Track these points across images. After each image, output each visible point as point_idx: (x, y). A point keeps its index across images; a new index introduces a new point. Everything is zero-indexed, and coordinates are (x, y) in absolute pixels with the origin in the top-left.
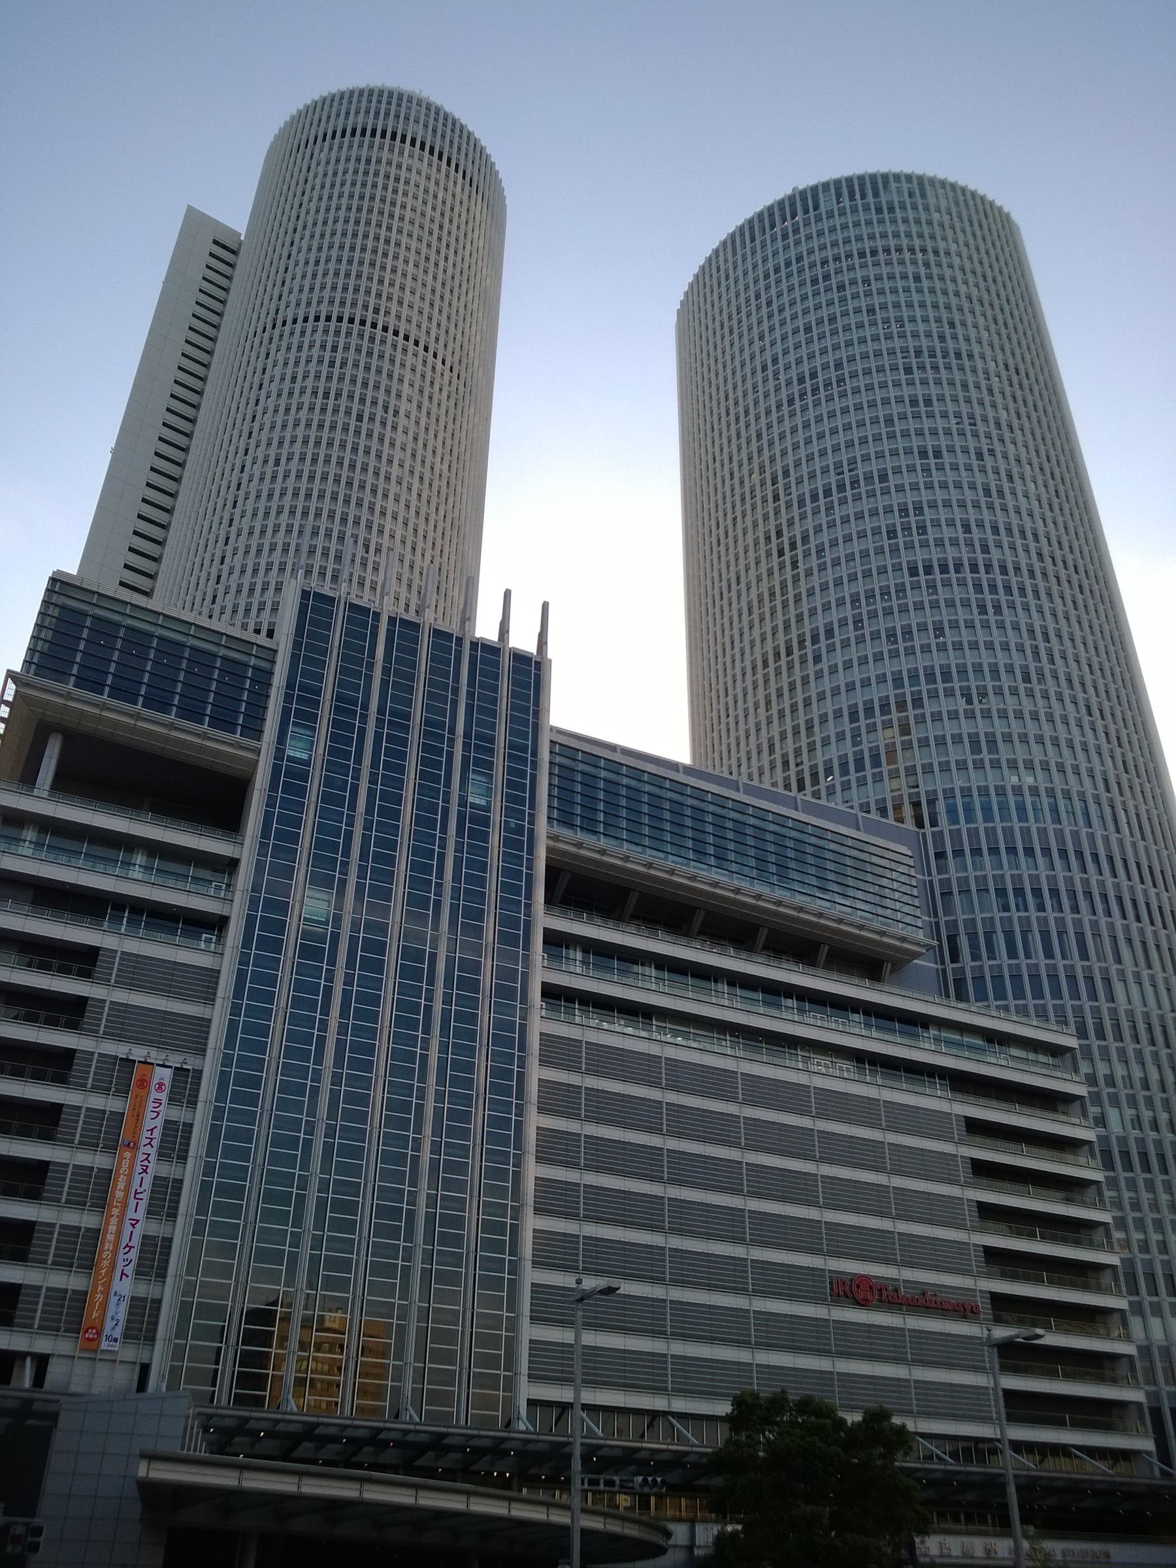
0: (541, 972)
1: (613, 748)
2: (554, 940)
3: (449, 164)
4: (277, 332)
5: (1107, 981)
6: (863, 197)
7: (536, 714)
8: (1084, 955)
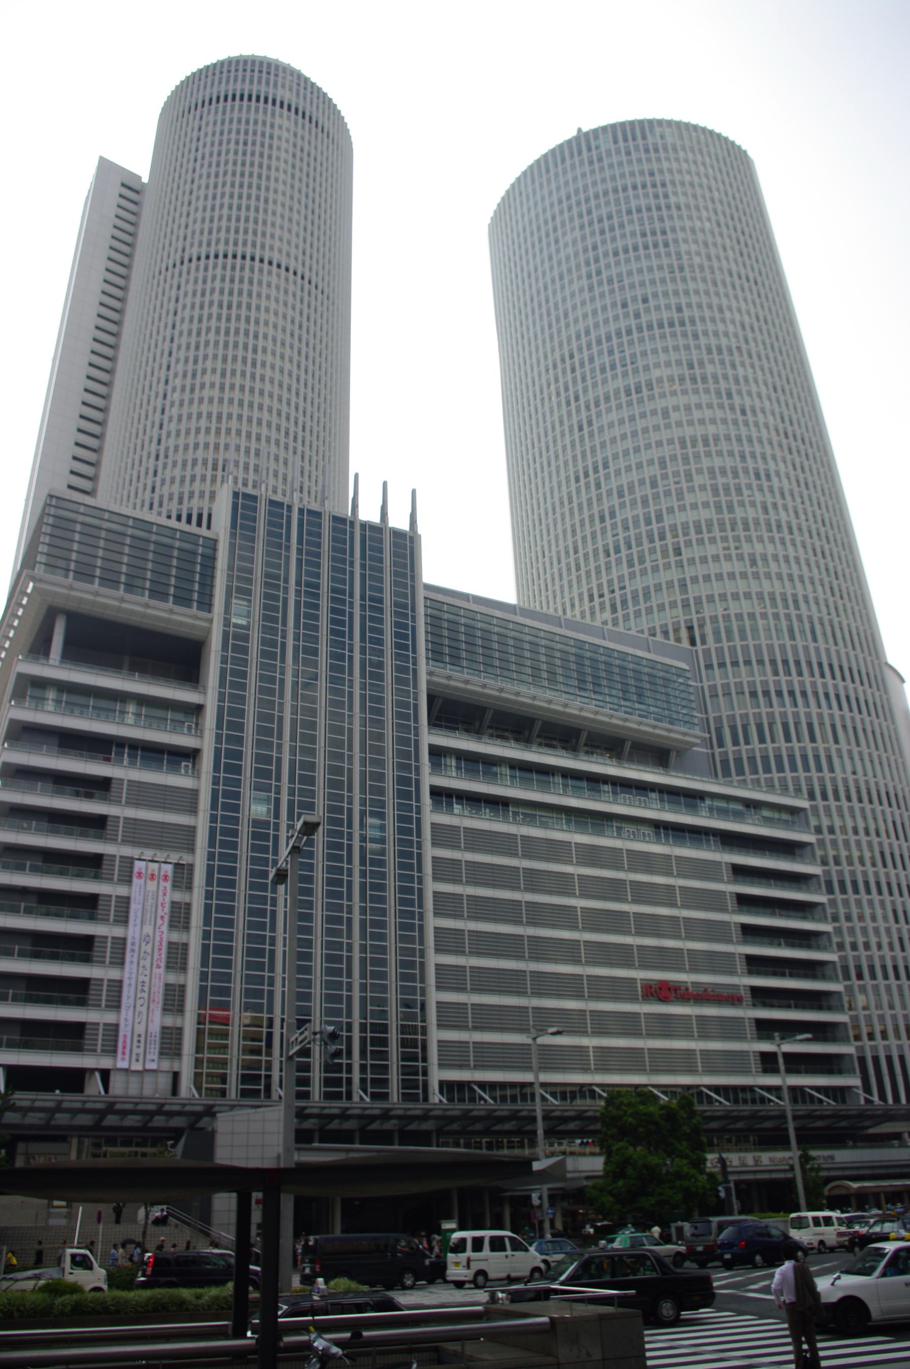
0: (428, 779)
1: (465, 597)
2: (437, 753)
4: (185, 268)
5: (829, 758)
6: (634, 139)
7: (413, 578)
8: (813, 739)
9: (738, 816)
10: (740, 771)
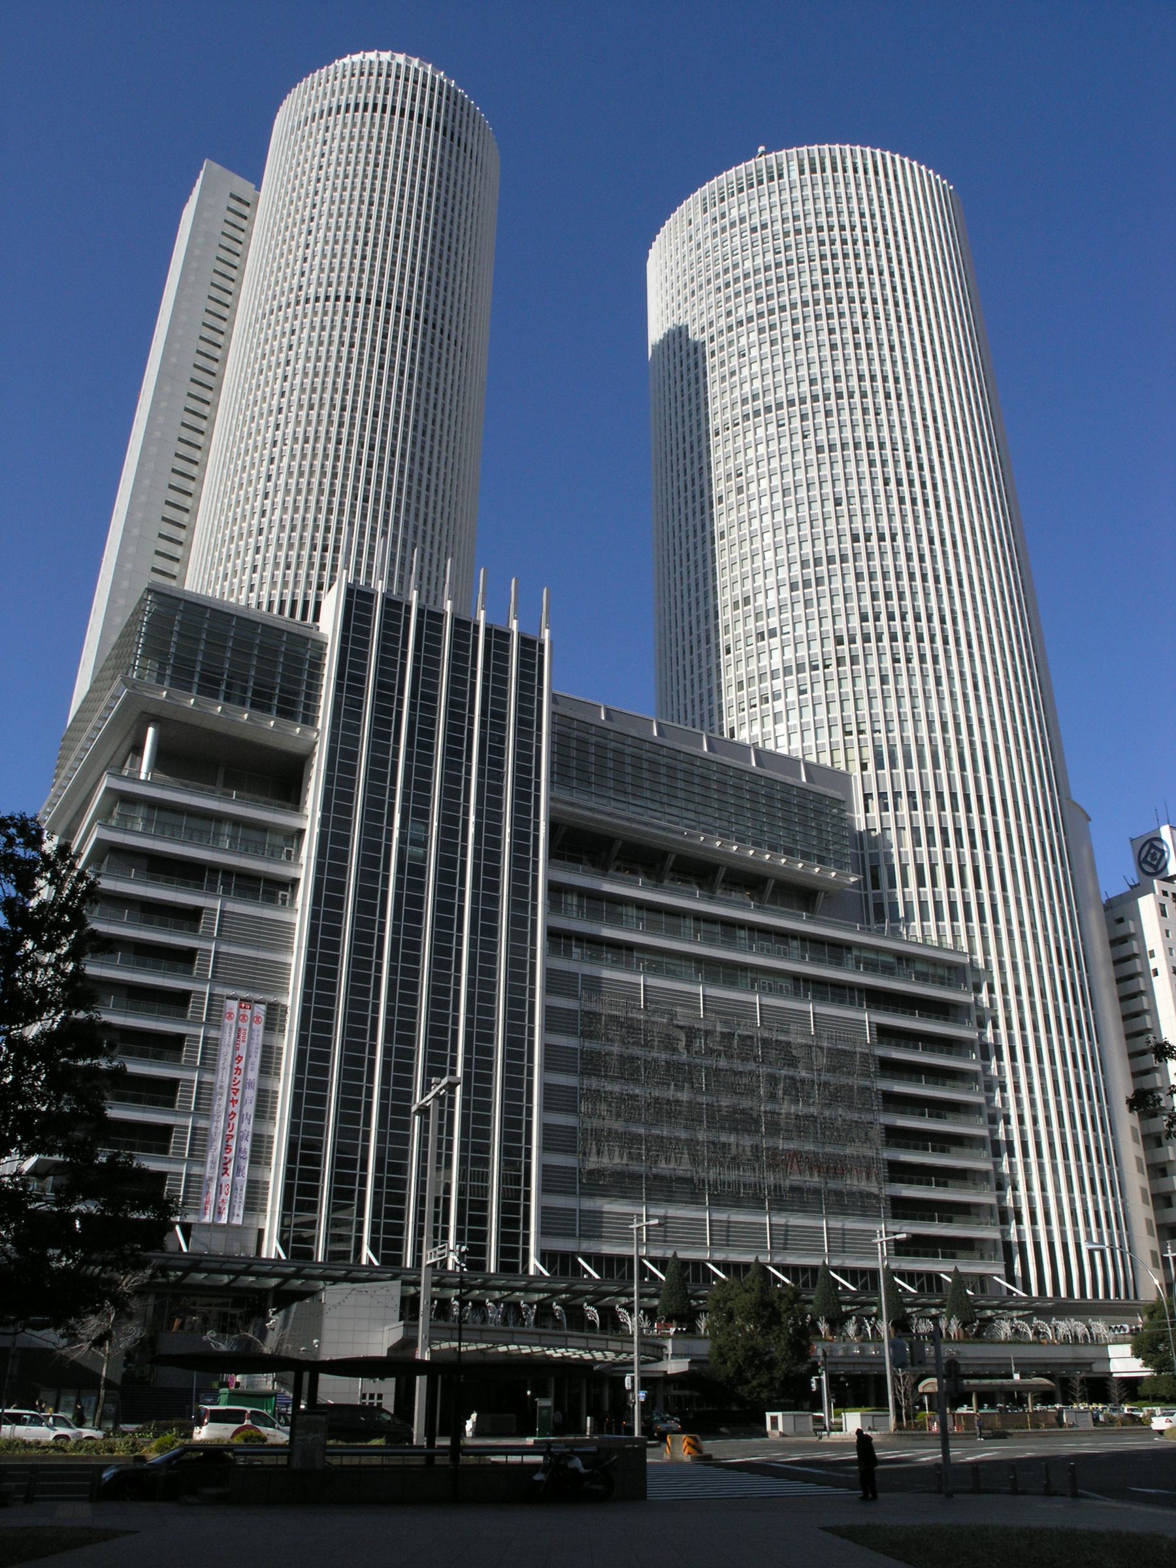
9: (887, 971)
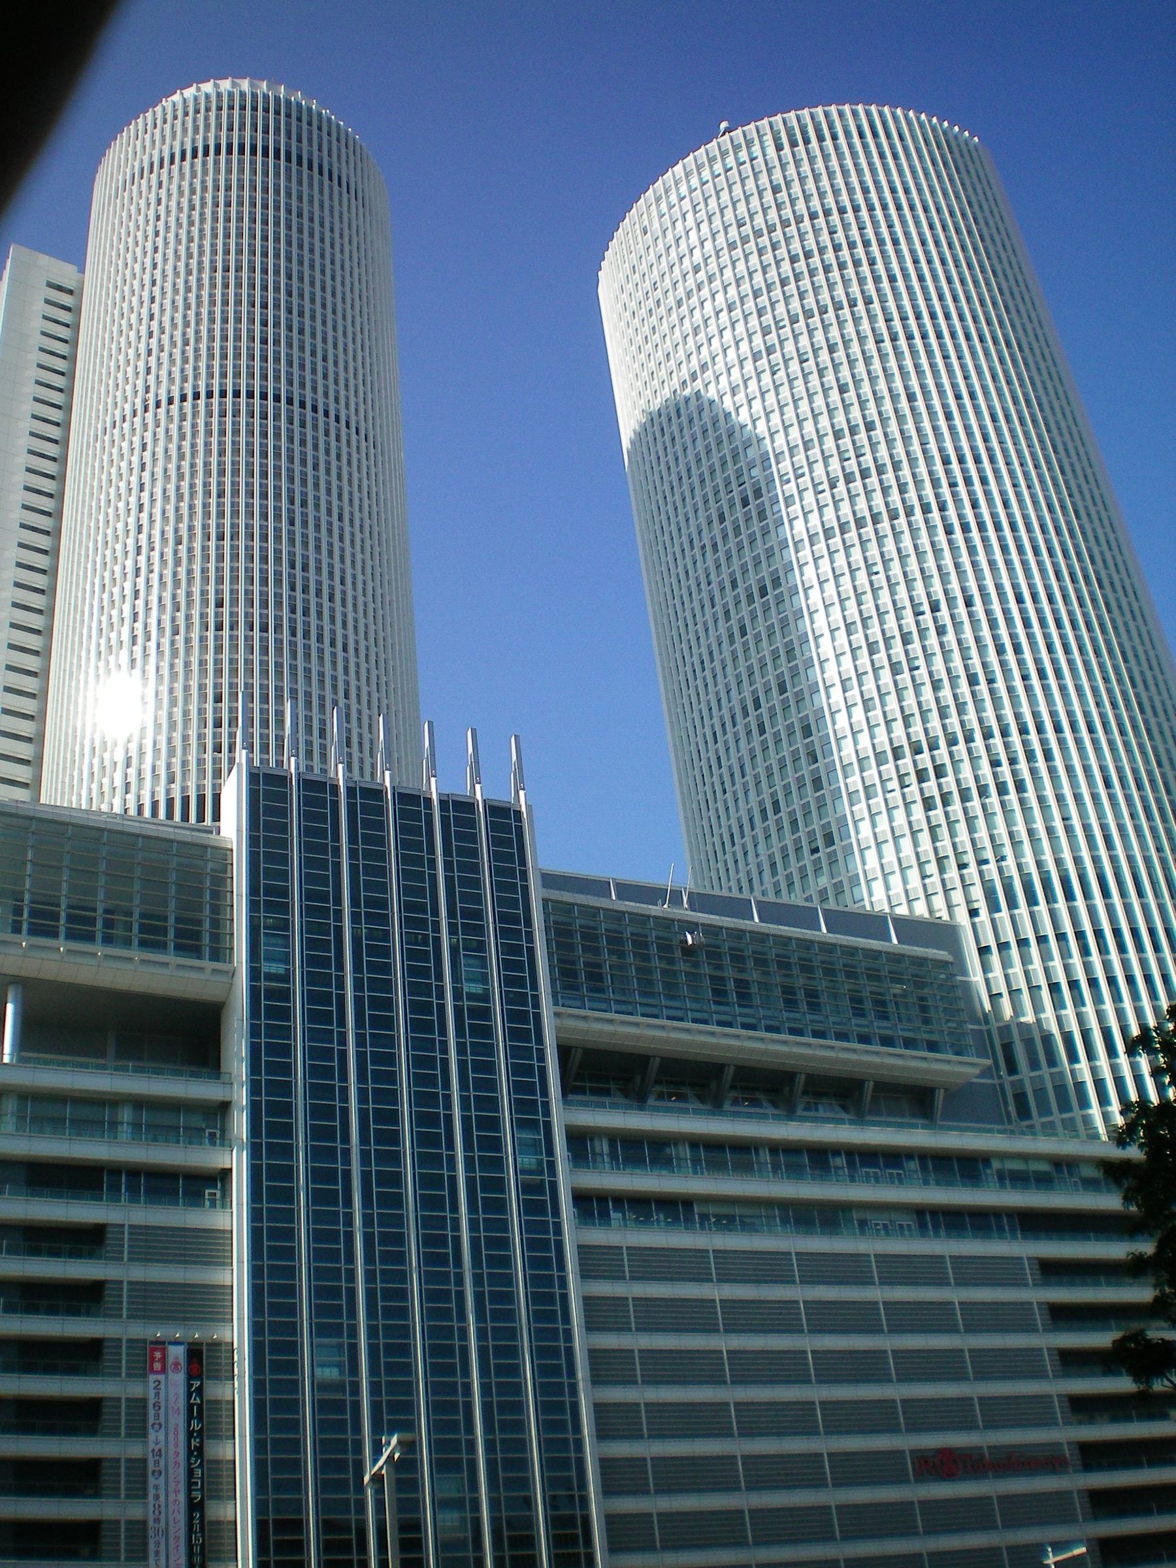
2: (579, 1140)
3: (321, 173)
9: (1043, 1181)
10: (1045, 1110)
